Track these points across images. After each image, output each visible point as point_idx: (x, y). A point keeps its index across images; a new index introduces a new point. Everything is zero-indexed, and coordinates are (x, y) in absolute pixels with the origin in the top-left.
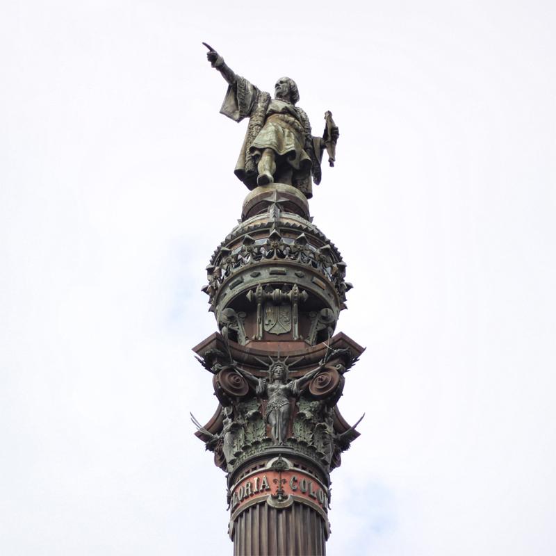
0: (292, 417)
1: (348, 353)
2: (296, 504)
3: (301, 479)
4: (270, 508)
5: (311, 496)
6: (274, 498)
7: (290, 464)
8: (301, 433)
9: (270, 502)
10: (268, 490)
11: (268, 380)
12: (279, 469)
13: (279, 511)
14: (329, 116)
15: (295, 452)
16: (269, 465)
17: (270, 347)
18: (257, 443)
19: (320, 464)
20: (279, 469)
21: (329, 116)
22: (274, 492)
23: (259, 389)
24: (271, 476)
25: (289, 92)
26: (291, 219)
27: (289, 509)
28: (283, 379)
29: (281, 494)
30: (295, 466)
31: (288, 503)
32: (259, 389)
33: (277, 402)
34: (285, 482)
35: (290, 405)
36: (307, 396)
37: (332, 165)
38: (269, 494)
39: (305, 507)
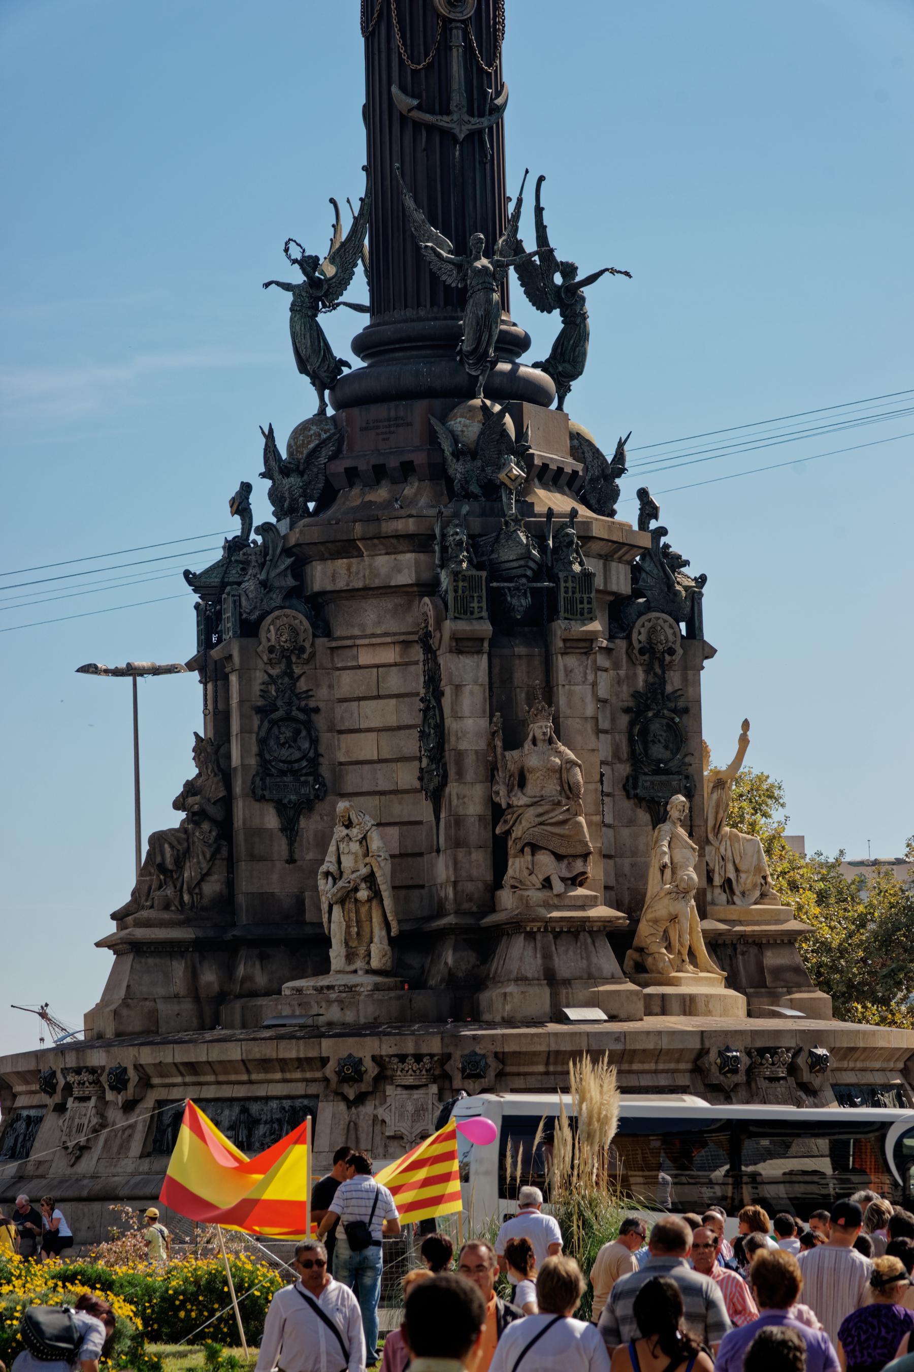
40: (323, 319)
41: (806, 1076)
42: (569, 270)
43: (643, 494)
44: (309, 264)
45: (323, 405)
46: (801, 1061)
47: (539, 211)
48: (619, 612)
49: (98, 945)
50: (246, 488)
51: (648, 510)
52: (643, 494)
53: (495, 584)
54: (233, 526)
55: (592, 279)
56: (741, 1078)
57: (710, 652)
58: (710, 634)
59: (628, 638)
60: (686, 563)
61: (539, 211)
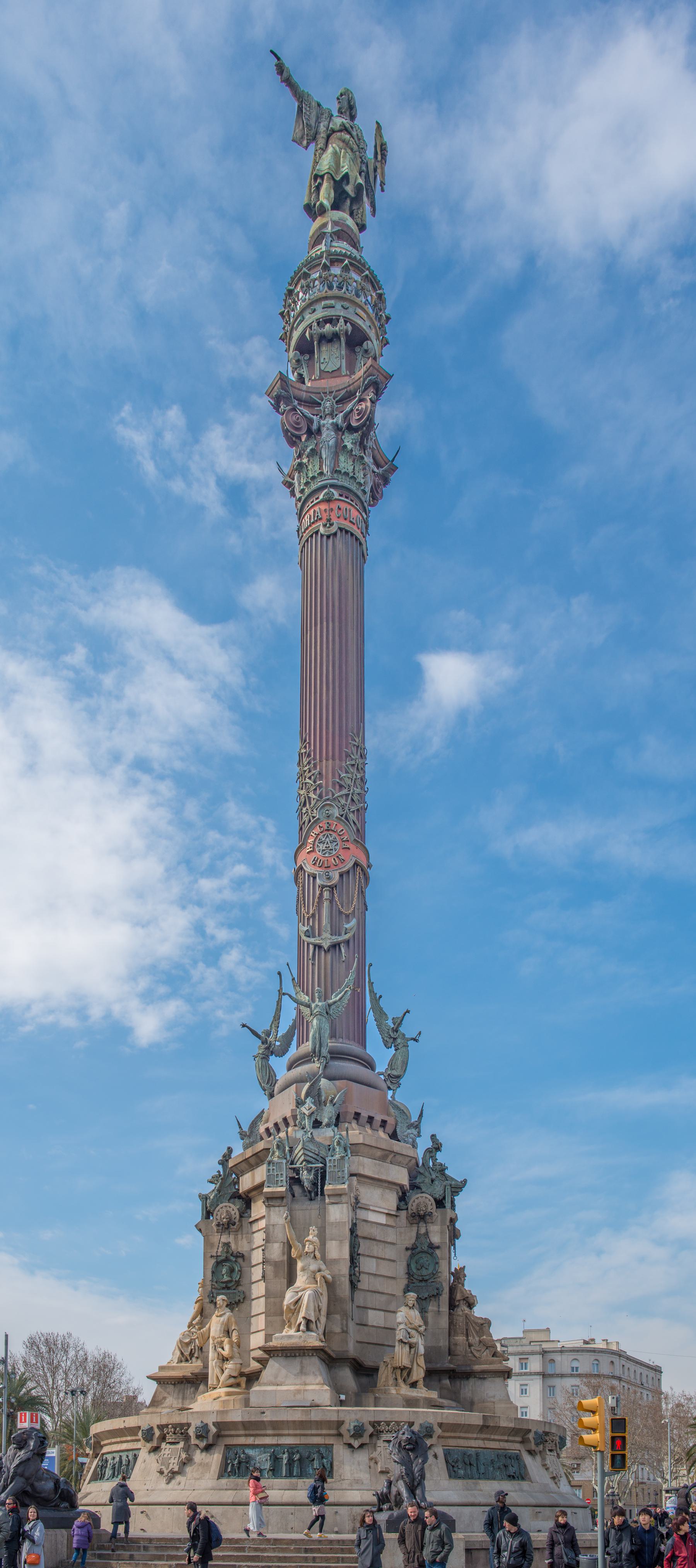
0: (340, 448)
2: (341, 529)
3: (343, 506)
4: (322, 536)
5: (351, 522)
6: (325, 526)
7: (336, 494)
8: (345, 464)
10: (321, 519)
11: (321, 417)
12: (328, 500)
13: (328, 537)
15: (340, 483)
17: (324, 384)
18: (313, 478)
19: (360, 493)
20: (328, 500)
22: (324, 521)
23: (315, 427)
24: (323, 507)
26: (341, 247)
27: (335, 534)
28: (332, 415)
30: (341, 495)
31: (334, 529)
32: (315, 427)
33: (328, 436)
34: (332, 510)
35: (337, 439)
36: (350, 429)
38: (320, 523)
47: (371, 984)
49: (148, 1377)
59: (407, 1209)
61: (371, 984)
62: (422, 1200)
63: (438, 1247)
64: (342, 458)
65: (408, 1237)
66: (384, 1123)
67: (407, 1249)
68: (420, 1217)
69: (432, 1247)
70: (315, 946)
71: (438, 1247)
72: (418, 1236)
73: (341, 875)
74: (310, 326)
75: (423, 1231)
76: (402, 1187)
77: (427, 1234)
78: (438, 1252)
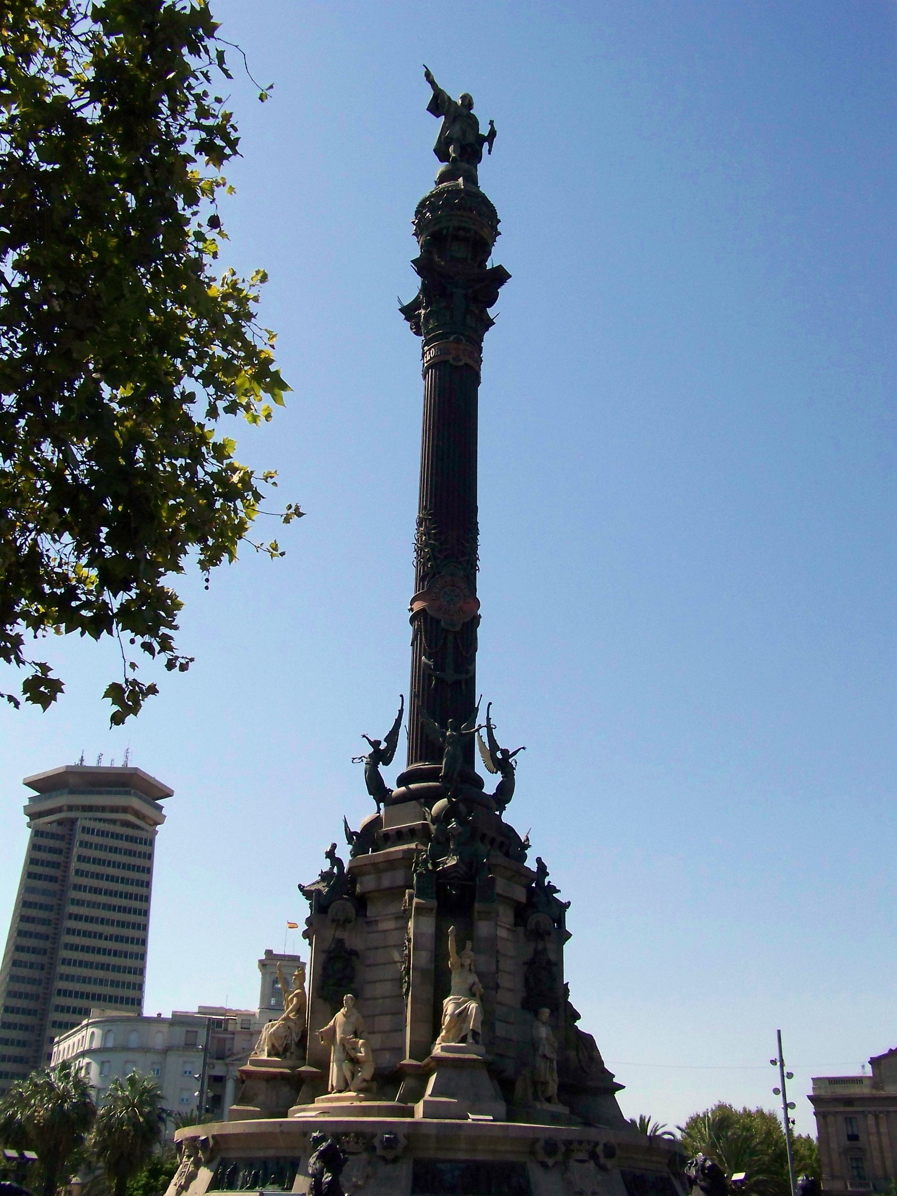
1: (500, 276)
2: (466, 364)
9: (452, 362)
14: (491, 123)
16: (452, 338)
21: (491, 123)
25: (468, 102)
29: (457, 359)
31: (461, 363)
37: (490, 153)
39: (471, 367)
40: (381, 768)
41: (602, 1160)
42: (505, 752)
43: (539, 860)
44: (375, 744)
45: (379, 809)
46: (599, 1150)
47: (488, 719)
48: (521, 913)
50: (334, 846)
51: (542, 869)
52: (539, 860)
53: (441, 881)
54: (326, 865)
55: (515, 753)
56: (559, 1157)
57: (569, 935)
58: (568, 928)
59: (525, 926)
60: (559, 891)
62: (538, 918)
63: (555, 964)
64: (468, 317)
65: (528, 951)
66: (502, 844)
67: (525, 963)
68: (538, 935)
69: (549, 962)
70: (437, 679)
71: (555, 964)
72: (535, 950)
73: (463, 624)
74: (448, 228)
75: (540, 947)
76: (519, 903)
77: (545, 950)
78: (555, 969)
